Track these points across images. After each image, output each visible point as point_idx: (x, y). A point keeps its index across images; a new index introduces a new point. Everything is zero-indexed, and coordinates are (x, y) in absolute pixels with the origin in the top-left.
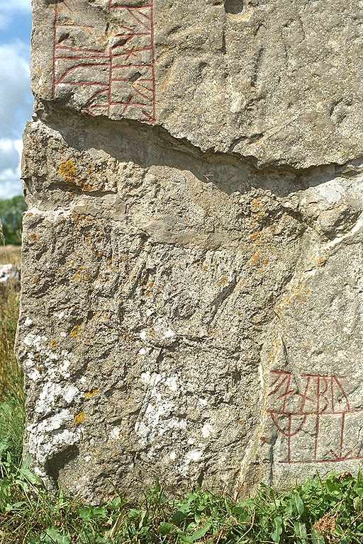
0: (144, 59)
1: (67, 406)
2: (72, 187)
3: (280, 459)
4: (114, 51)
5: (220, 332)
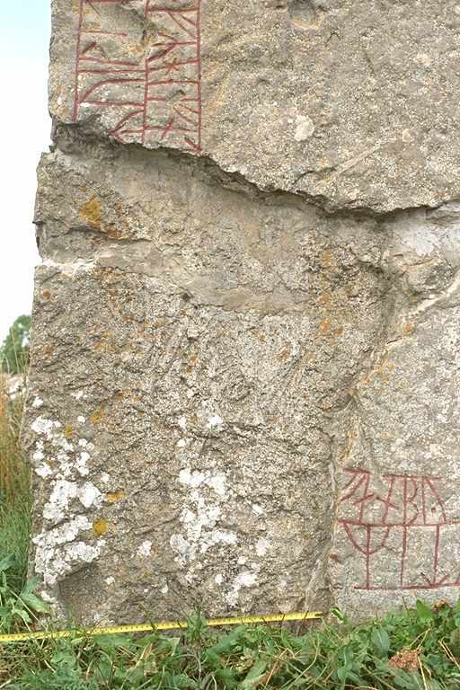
0: (188, 74)
1: (87, 512)
2: (98, 233)
3: (356, 584)
4: (151, 64)
5: (281, 420)
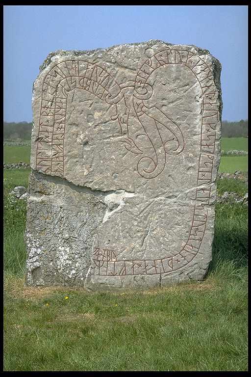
2: (41, 193)
